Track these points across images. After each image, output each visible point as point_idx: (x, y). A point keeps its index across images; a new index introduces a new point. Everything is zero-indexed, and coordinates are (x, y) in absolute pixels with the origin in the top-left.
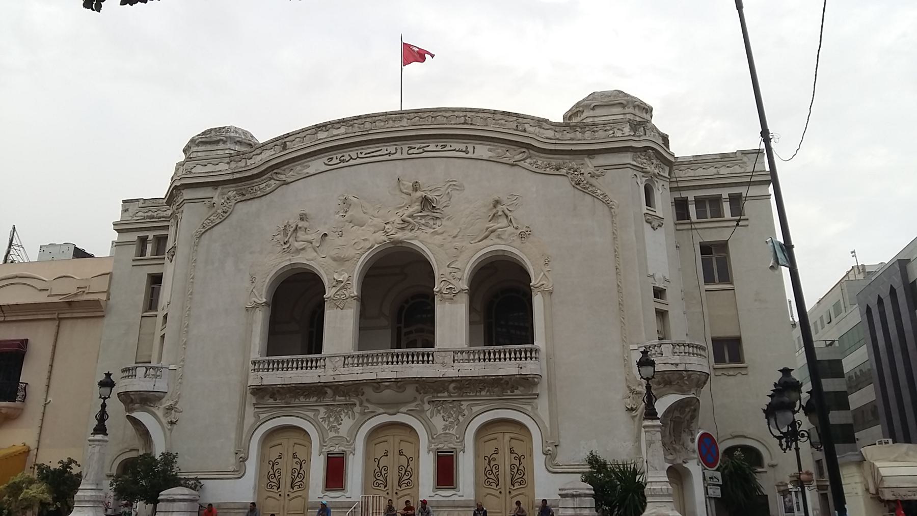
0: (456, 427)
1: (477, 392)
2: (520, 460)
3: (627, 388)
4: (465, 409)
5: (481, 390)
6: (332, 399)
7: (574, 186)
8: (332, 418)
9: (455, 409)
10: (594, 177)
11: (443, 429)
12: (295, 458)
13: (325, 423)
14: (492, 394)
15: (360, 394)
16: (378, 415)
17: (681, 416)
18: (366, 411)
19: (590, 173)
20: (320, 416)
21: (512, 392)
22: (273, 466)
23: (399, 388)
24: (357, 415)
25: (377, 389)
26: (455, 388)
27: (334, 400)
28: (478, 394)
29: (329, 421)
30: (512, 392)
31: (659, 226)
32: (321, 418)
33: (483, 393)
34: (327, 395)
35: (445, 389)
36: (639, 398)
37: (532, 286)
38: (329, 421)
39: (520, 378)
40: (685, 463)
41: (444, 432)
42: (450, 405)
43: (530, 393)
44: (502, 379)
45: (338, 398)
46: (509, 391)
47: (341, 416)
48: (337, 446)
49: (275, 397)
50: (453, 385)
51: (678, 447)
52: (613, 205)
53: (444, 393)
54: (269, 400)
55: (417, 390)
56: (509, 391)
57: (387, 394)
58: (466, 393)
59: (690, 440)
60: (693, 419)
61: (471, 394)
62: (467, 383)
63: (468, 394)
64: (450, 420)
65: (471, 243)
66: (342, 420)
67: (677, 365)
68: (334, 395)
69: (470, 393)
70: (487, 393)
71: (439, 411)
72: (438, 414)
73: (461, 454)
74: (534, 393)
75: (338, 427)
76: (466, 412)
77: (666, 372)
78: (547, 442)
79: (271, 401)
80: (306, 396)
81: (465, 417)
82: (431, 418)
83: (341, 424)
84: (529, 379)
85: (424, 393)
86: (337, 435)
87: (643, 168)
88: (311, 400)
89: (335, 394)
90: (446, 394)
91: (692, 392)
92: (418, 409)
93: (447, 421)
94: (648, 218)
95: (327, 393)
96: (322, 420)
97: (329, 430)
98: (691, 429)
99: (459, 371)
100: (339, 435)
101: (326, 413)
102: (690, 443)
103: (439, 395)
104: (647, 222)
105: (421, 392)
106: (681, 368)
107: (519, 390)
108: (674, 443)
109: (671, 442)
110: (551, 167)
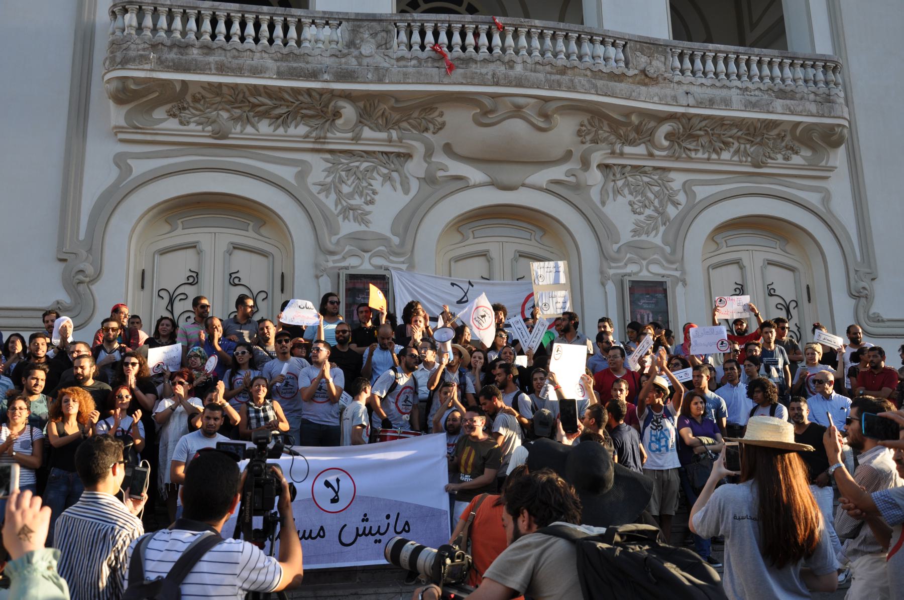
0: (662, 229)
1: (714, 150)
2: (788, 312)
4: (679, 190)
5: (727, 144)
6: (350, 135)
8: (350, 186)
9: (657, 189)
11: (634, 231)
12: (236, 285)
13: (327, 197)
14: (744, 159)
15: (431, 126)
16: (475, 186)
18: (440, 174)
20: (311, 180)
21: (787, 159)
22: (171, 302)
23: (546, 116)
24: (414, 185)
25: (486, 113)
26: (668, 137)
27: (356, 139)
28: (714, 156)
29: (339, 192)
30: (787, 159)
32: (314, 184)
33: (726, 155)
34: (339, 122)
35: (648, 137)
38: (339, 192)
41: (636, 238)
42: (646, 179)
43: (823, 163)
45: (367, 133)
46: (779, 156)
47: (372, 182)
48: (367, 255)
49: (185, 114)
50: (666, 128)
53: (639, 144)
54: (165, 120)
55: (579, 133)
56: (779, 156)
57: (517, 127)
58: (690, 150)
61: (700, 155)
62: (704, 123)
63: (693, 155)
64: (648, 212)
66: (375, 193)
68: (356, 126)
69: (696, 151)
70: (732, 156)
71: (618, 192)
72: (620, 198)
73: (679, 288)
74: (830, 164)
75: (368, 208)
76: (681, 198)
78: (856, 271)
79: (172, 124)
80: (278, 117)
81: (680, 207)
82: (603, 203)
83: (372, 202)
84: (836, 129)
85: (595, 141)
86: (363, 228)
88: (292, 130)
89: (361, 121)
90: (641, 150)
92: (572, 179)
93: (640, 213)
95: (337, 114)
96: (320, 187)
97: (340, 213)
99: (687, 93)
100: (373, 228)
101: (329, 171)
103: (628, 149)
105: (588, 138)
107: (803, 157)
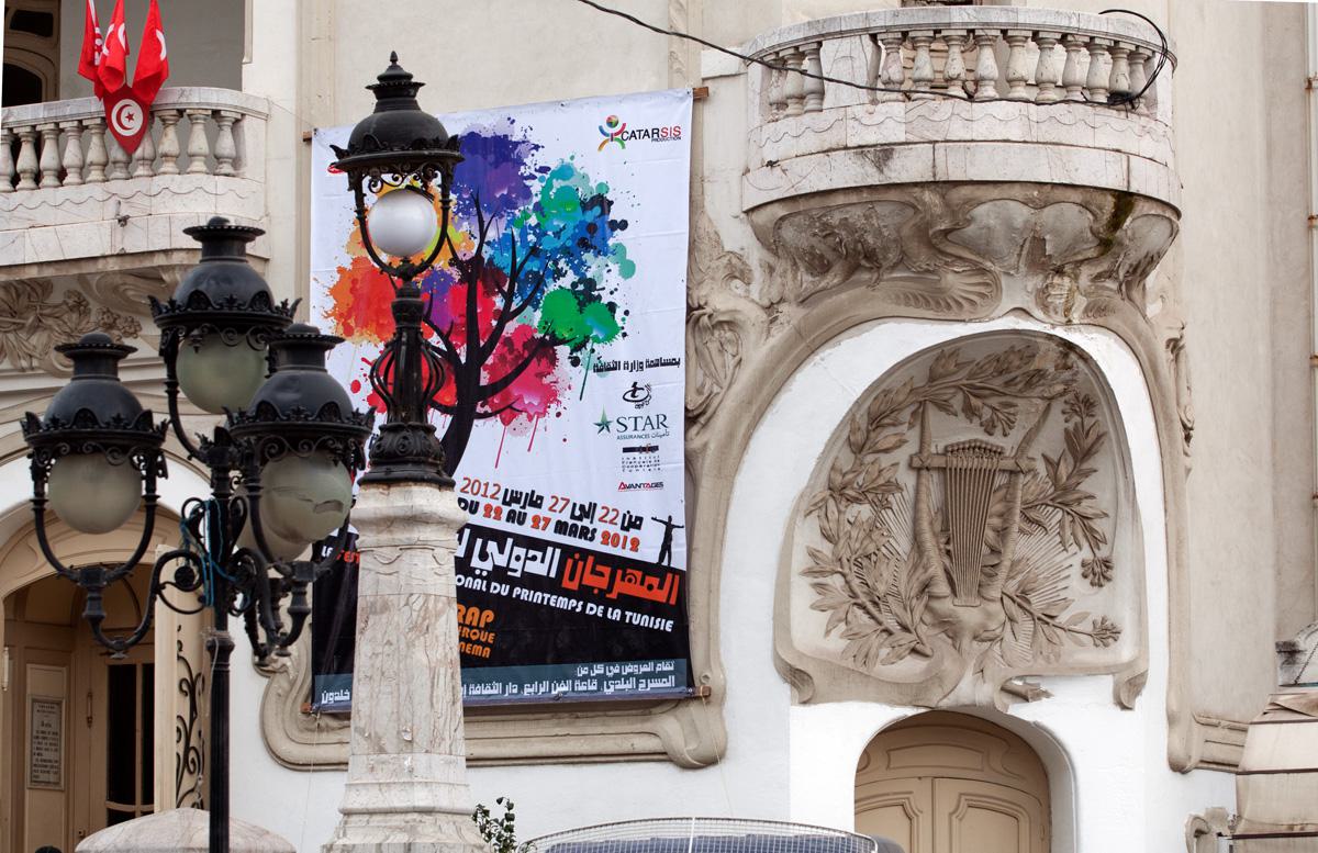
17: (996, 440)
36: (722, 350)
39: (123, 273)
40: (1023, 697)
44: (44, 286)
51: (970, 615)
59: (1077, 570)
60: (1088, 453)
67: (883, 153)
77: (840, 200)
91: (1007, 303)
98: (1085, 507)
102: (1077, 586)
106: (909, 167)
108: (942, 588)
109: (925, 587)
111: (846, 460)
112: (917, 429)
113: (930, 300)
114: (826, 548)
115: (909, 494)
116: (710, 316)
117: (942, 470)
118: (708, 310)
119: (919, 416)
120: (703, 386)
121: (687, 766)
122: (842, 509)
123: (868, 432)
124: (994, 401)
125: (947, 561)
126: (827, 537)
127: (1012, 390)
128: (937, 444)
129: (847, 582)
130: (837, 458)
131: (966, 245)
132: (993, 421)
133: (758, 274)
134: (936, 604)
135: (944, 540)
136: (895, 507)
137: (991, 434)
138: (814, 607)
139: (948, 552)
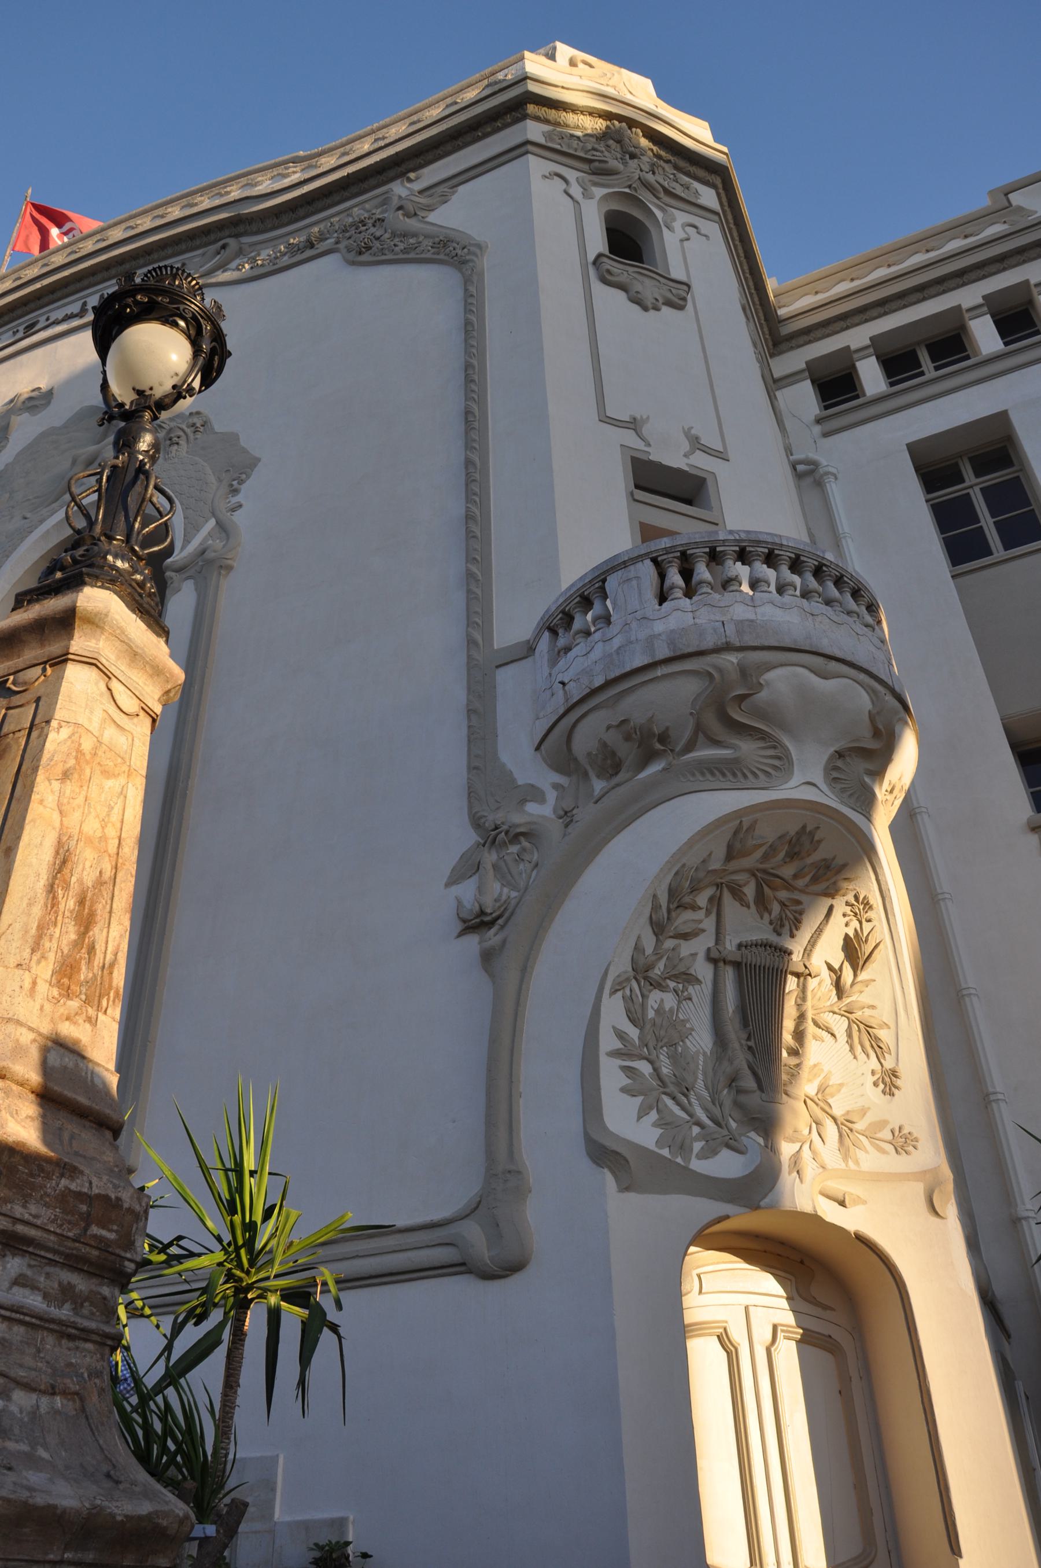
3: (472, 838)
7: (353, 263)
10: (415, 214)
19: (400, 208)
31: (669, 303)
37: (168, 568)
52: (470, 253)
65: (25, 518)
87: (590, 161)
91: (797, 779)
94: (609, 267)
104: (604, 281)
108: (750, 1083)
110: (296, 249)
111: (649, 943)
112: (713, 916)
113: (726, 772)
114: (633, 1033)
115: (707, 987)
116: (507, 833)
117: (737, 965)
118: (505, 827)
119: (716, 903)
120: (500, 894)
121: (488, 1276)
122: (646, 993)
123: (669, 911)
124: (783, 895)
125: (751, 1058)
126: (633, 1021)
127: (800, 883)
128: (730, 945)
129: (655, 1069)
130: (639, 937)
131: (761, 714)
132: (781, 919)
133: (551, 796)
134: (742, 1098)
135: (745, 1036)
136: (695, 999)
137: (779, 934)
138: (624, 1090)
139: (750, 1048)
